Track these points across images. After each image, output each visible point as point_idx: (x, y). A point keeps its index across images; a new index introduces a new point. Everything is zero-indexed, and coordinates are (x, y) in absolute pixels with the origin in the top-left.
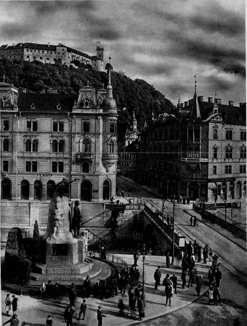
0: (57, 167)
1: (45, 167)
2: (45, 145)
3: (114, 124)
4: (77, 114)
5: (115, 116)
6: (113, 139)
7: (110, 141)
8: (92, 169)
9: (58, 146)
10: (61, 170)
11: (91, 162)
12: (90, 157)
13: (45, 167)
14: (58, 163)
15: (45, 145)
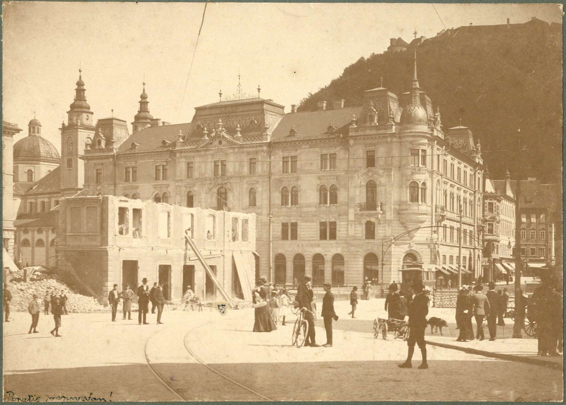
0: (328, 232)
1: (309, 230)
2: (309, 195)
3: (419, 150)
4: (355, 138)
5: (424, 137)
6: (417, 178)
7: (411, 181)
8: (380, 232)
9: (328, 195)
10: (333, 236)
11: (377, 218)
12: (375, 210)
13: (309, 230)
14: (328, 223)
15: (309, 195)
